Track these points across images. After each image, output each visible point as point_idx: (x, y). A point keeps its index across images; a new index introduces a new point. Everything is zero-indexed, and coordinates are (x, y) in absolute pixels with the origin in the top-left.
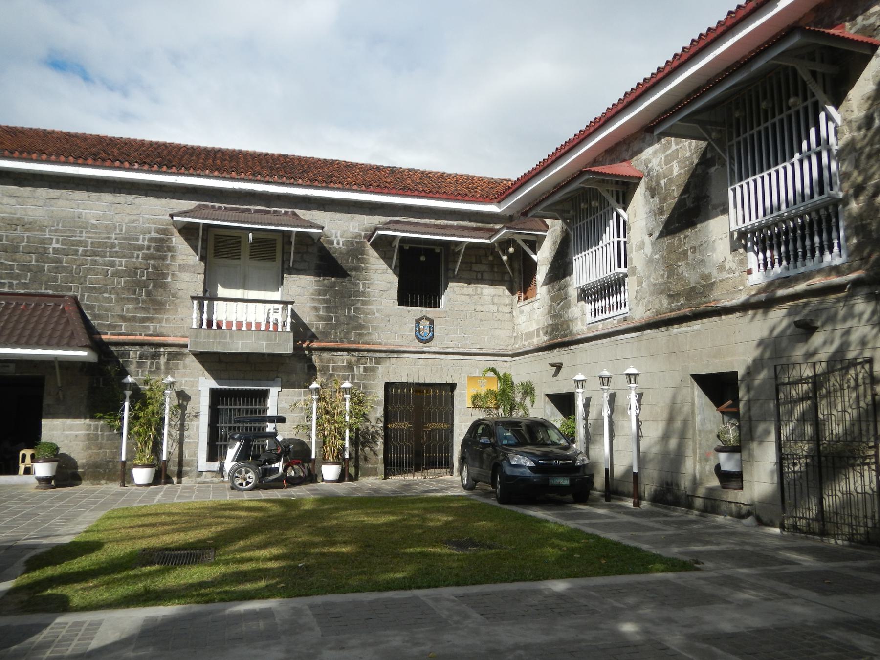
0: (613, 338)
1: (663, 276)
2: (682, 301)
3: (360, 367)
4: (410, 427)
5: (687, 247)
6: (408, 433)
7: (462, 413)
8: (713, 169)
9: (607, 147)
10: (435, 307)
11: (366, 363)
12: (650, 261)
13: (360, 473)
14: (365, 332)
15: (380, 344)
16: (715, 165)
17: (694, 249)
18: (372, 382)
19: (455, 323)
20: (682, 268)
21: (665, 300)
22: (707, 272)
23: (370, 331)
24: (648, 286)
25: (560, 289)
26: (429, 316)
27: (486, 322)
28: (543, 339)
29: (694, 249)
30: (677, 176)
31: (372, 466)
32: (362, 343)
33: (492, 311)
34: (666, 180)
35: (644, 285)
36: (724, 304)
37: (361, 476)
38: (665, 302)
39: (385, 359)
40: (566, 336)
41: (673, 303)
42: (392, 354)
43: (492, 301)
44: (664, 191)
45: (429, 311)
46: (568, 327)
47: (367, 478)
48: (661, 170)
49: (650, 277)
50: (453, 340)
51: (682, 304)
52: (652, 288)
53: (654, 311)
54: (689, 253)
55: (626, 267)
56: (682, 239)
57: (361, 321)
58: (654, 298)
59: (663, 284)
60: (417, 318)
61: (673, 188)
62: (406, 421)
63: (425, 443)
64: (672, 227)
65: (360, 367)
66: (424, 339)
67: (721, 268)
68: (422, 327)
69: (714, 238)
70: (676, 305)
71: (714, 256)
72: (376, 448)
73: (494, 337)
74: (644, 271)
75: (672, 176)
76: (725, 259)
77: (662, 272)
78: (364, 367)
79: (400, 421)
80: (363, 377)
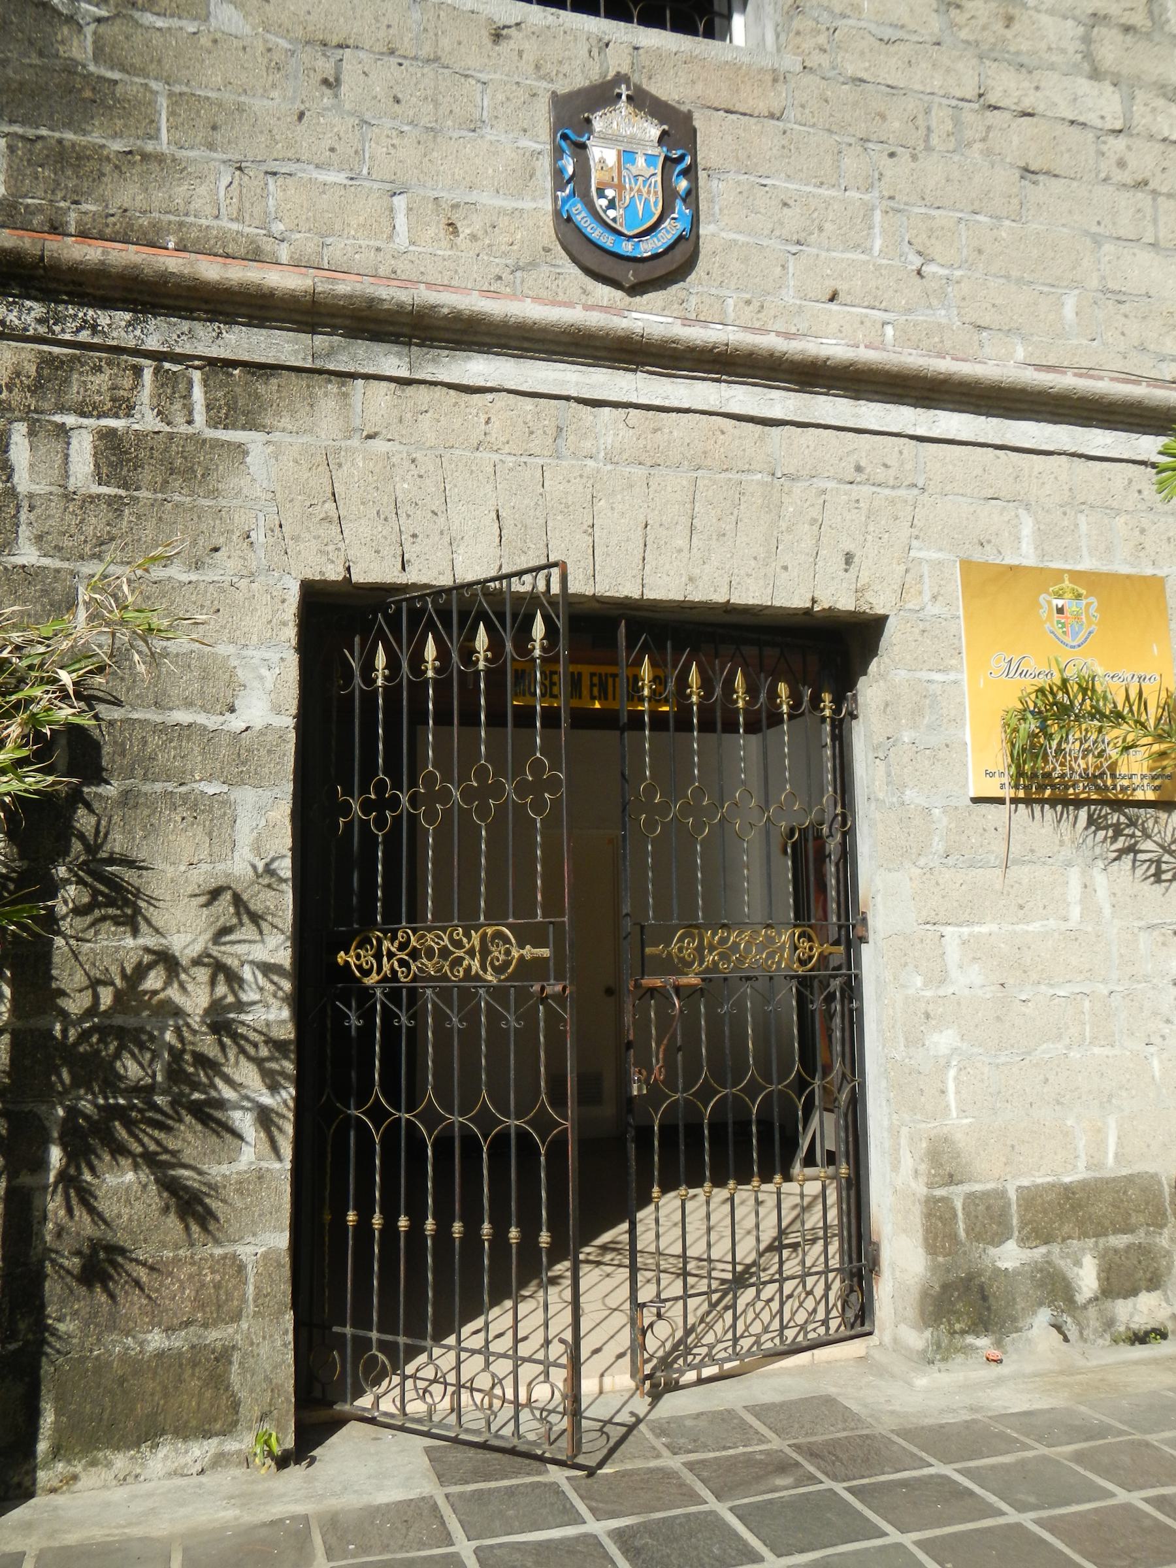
3: (63, 432)
4: (529, 969)
6: (512, 1022)
7: (938, 846)
10: (709, 34)
11: (123, 406)
13: (48, 1419)
14: (117, 146)
15: (255, 256)
18: (177, 573)
19: (850, 163)
23: (164, 144)
26: (665, 89)
27: (1057, 186)
31: (179, 1341)
32: (83, 234)
33: (1092, 118)
37: (57, 1452)
39: (303, 381)
42: (361, 348)
43: (1088, 56)
45: (658, 54)
47: (121, 1461)
50: (842, 286)
57: (80, 49)
60: (564, 87)
62: (496, 914)
63: (655, 1095)
65: (63, 432)
66: (627, 248)
68: (602, 154)
72: (217, 1171)
73: (1120, 298)
78: (108, 437)
79: (443, 914)
80: (96, 523)
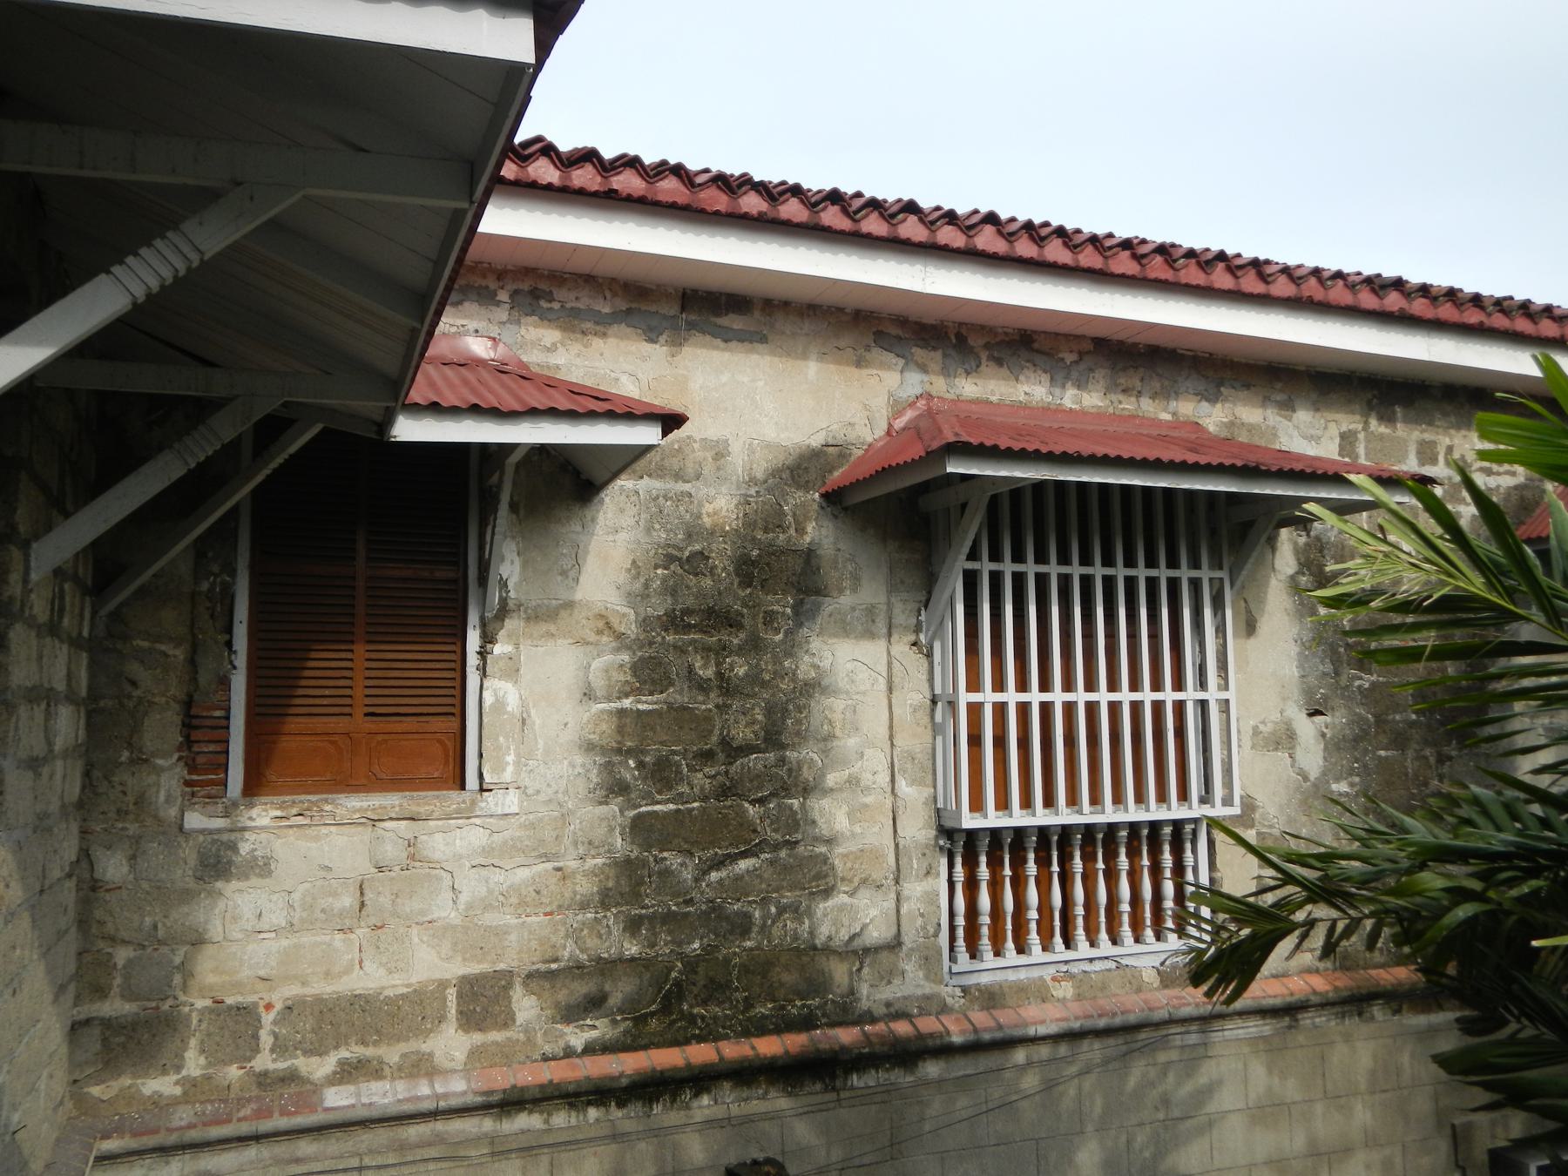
12: (1316, 795)
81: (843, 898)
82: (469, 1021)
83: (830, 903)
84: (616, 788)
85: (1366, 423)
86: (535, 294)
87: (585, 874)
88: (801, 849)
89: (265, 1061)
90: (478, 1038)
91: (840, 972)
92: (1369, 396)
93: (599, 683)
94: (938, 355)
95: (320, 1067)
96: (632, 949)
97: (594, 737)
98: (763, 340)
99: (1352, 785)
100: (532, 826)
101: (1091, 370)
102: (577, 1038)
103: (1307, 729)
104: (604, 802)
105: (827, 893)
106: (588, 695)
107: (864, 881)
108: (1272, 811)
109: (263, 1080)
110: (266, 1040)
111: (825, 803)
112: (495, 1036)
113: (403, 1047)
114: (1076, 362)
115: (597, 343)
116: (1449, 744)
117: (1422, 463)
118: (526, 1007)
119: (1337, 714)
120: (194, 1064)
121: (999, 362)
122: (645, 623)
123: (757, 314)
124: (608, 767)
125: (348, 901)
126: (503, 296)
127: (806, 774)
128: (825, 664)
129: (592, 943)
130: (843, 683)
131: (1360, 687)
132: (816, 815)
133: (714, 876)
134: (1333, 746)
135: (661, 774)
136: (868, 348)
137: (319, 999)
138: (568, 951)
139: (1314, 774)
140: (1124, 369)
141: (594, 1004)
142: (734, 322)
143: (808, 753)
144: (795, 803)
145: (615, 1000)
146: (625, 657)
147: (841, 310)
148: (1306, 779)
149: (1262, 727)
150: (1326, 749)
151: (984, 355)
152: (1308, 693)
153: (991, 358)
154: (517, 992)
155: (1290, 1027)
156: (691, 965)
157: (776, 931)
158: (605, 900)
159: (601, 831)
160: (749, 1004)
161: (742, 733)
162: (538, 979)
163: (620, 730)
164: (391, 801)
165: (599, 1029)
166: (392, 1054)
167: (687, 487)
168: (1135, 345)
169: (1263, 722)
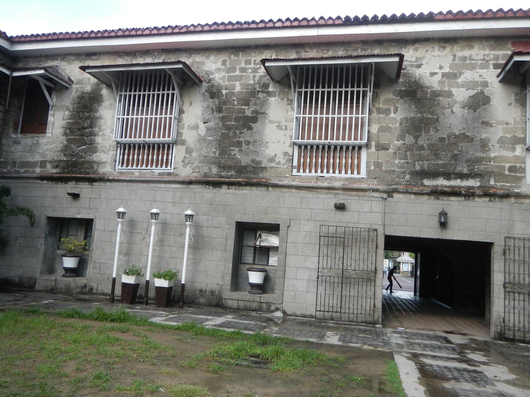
0: (154, 185)
1: (215, 153)
2: (233, 173)
5: (241, 139)
8: (272, 99)
9: (164, 48)
12: (202, 140)
16: (275, 97)
17: (248, 143)
20: (235, 151)
21: (215, 169)
22: (258, 160)
24: (199, 156)
25: (82, 135)
28: (50, 170)
29: (248, 143)
30: (238, 92)
34: (227, 91)
35: (194, 154)
36: (277, 182)
38: (215, 170)
40: (88, 173)
41: (223, 172)
44: (224, 98)
46: (92, 167)
48: (222, 83)
49: (201, 150)
51: (232, 175)
52: (202, 158)
53: (202, 173)
54: (243, 144)
55: (169, 137)
56: (238, 133)
58: (203, 165)
59: (213, 157)
61: (234, 99)
64: (229, 123)
67: (272, 160)
69: (268, 140)
70: (226, 174)
71: (267, 151)
74: (195, 145)
75: (234, 91)
76: (276, 155)
77: (215, 150)
81: (98, 154)
82: (41, 167)
83: (96, 154)
84: (66, 134)
85: (230, 58)
86: (64, 58)
87: (60, 147)
88: (93, 145)
89: (16, 169)
90: (42, 169)
91: (95, 166)
92: (232, 51)
93: (65, 117)
94: (130, 57)
95: (22, 170)
96: (65, 159)
97: (64, 126)
98: (98, 59)
99: (213, 138)
100: (53, 139)
101: (161, 56)
102: (54, 171)
103: (202, 126)
104: (63, 136)
105: (96, 152)
106: (63, 119)
107: (103, 151)
108: (190, 143)
109: (16, 171)
110: (17, 166)
111: (98, 138)
112: (44, 169)
113: (32, 169)
114: (158, 55)
115: (72, 64)
116: (244, 129)
117: (246, 65)
118: (48, 166)
119: (211, 122)
120: (9, 168)
121: (141, 57)
122: (74, 108)
123: (98, 55)
124: (65, 131)
125: (29, 148)
126: (59, 59)
127: (96, 133)
128: (102, 114)
129: (59, 157)
130: (104, 117)
131: (219, 117)
132: (96, 139)
133: (79, 148)
134: (208, 129)
135: (72, 132)
136: (116, 58)
137: (23, 161)
138: (56, 158)
139: (202, 135)
140: (168, 54)
141: (57, 166)
142: (94, 57)
143: (96, 129)
144: (93, 137)
145: (60, 166)
146: (70, 113)
147: (112, 52)
148: (200, 136)
149: (190, 125)
150: (207, 129)
151: (138, 56)
152: (204, 118)
153: (140, 56)
154: (48, 163)
155: (187, 187)
156: (73, 162)
157: (87, 158)
158: (62, 151)
159: (63, 140)
160: (80, 169)
161: (86, 125)
162: (51, 162)
163: (68, 125)
164: (35, 135)
165: (58, 170)
166: (30, 170)
167: (83, 86)
168: (171, 49)
169: (191, 124)
